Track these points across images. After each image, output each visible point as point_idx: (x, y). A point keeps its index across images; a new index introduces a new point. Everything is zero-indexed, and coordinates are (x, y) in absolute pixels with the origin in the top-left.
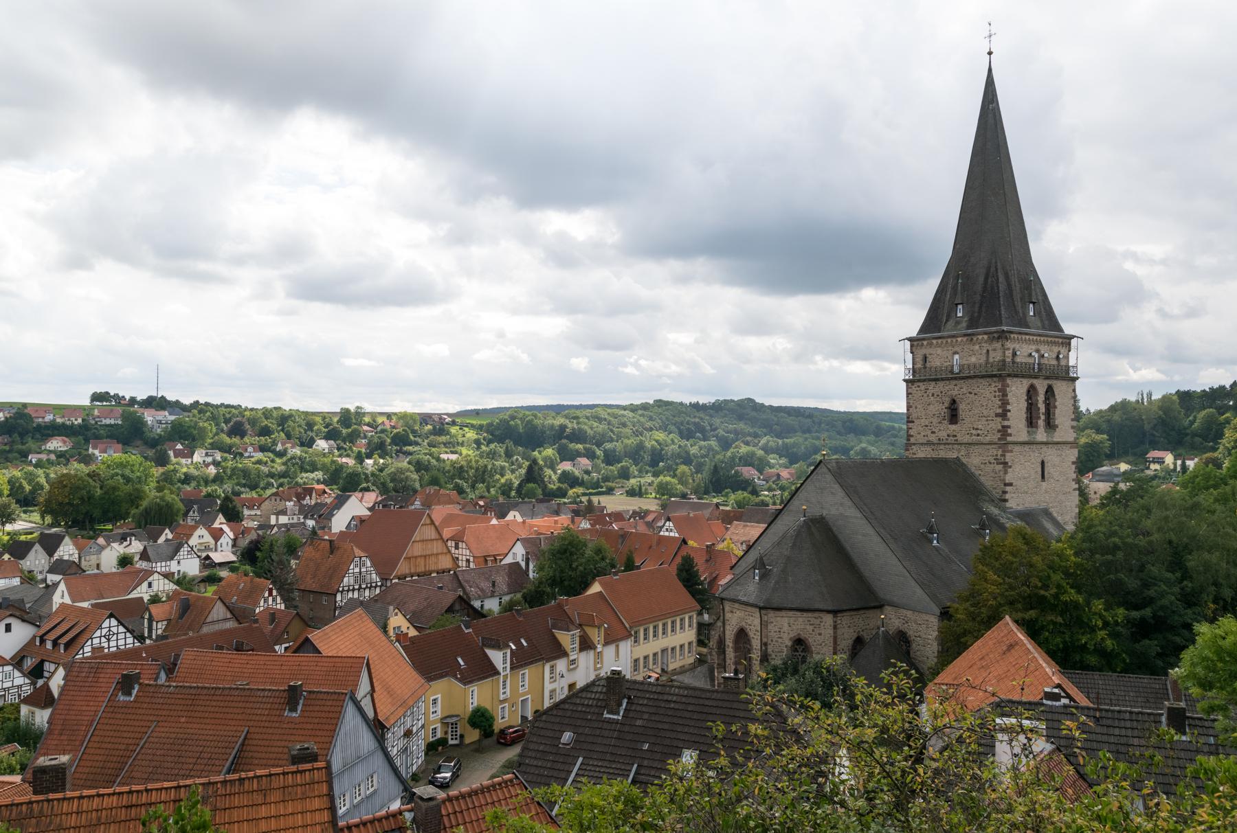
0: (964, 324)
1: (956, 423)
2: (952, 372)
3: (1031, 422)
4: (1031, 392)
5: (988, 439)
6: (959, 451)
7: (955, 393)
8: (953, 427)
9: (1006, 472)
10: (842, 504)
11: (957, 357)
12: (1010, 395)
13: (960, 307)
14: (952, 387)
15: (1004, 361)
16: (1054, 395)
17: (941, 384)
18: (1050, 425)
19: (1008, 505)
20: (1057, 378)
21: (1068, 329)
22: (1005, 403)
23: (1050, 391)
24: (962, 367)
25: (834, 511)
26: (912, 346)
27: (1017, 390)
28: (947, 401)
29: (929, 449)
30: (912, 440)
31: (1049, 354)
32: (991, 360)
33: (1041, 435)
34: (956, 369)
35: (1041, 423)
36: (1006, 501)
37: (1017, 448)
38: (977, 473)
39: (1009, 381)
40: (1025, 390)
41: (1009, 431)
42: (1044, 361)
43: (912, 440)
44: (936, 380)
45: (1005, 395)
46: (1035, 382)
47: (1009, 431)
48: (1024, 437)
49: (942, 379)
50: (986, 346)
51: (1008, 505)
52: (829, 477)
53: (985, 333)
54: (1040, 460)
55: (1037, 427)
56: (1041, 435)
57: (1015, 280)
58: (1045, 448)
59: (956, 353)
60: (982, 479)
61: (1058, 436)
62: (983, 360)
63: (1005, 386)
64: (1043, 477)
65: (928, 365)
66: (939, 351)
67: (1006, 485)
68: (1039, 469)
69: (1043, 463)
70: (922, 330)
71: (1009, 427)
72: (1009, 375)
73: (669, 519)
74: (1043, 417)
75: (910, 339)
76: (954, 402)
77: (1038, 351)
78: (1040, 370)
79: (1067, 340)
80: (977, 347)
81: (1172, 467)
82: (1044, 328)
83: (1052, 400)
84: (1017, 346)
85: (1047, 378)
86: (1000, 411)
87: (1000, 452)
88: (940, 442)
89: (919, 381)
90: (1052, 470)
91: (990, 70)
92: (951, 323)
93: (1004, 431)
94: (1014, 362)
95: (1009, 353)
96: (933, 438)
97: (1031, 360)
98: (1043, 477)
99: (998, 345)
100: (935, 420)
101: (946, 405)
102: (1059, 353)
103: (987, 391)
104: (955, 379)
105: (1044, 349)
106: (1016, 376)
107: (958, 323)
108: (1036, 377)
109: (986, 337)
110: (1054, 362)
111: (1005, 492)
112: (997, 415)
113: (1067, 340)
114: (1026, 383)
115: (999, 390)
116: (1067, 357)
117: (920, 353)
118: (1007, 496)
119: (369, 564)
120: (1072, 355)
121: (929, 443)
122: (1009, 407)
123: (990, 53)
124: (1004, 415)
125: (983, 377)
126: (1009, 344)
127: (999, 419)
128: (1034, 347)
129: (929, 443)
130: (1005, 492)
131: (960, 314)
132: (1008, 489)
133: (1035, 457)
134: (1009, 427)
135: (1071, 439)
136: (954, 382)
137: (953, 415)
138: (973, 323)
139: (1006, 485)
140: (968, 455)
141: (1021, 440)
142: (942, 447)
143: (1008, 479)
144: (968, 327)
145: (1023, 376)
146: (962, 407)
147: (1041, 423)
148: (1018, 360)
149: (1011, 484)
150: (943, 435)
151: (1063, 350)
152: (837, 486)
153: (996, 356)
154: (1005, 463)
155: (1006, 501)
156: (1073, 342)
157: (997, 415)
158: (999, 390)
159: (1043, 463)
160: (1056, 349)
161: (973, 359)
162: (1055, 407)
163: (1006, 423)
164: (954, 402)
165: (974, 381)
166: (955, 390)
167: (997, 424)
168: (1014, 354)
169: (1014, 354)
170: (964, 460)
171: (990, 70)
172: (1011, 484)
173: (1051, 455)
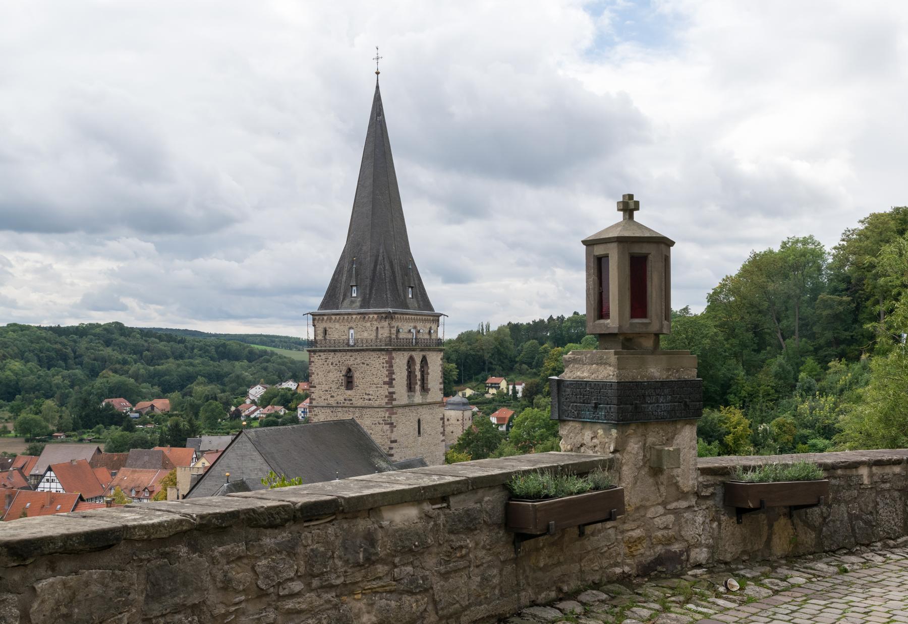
0: (358, 304)
1: (351, 389)
2: (348, 345)
3: (410, 388)
4: (411, 362)
5: (377, 403)
6: (354, 413)
7: (350, 363)
8: (349, 392)
9: (392, 432)
10: (260, 470)
11: (352, 331)
12: (395, 366)
13: (354, 288)
14: (348, 357)
15: (390, 337)
16: (427, 363)
17: (339, 354)
18: (425, 389)
19: (393, 459)
20: (429, 350)
21: (437, 311)
22: (391, 373)
24: (356, 341)
25: (253, 476)
26: (314, 320)
27: (400, 361)
28: (344, 369)
29: (328, 411)
30: (314, 403)
31: (423, 328)
32: (380, 336)
33: (418, 398)
34: (351, 343)
35: (418, 387)
36: (392, 455)
37: (400, 411)
38: (369, 432)
39: (394, 354)
40: (405, 361)
41: (394, 396)
42: (420, 336)
43: (314, 403)
44: (335, 351)
45: (391, 366)
46: (413, 353)
47: (394, 396)
49: (340, 351)
50: (376, 324)
51: (393, 459)
52: (249, 446)
53: (375, 313)
55: (414, 391)
56: (418, 398)
57: (397, 269)
58: (420, 409)
59: (351, 328)
60: (373, 437)
62: (373, 336)
63: (392, 358)
64: (419, 432)
65: (328, 337)
66: (337, 326)
67: (392, 442)
69: (419, 421)
70: (324, 306)
71: (394, 393)
72: (394, 350)
73: (50, 469)
74: (419, 383)
75: (313, 315)
76: (349, 370)
77: (415, 327)
79: (436, 318)
80: (368, 324)
81: (505, 391)
82: (420, 308)
83: (425, 368)
84: (400, 324)
85: (422, 350)
86: (387, 379)
87: (387, 415)
88: (338, 406)
89: (320, 351)
91: (378, 87)
92: (347, 301)
93: (391, 396)
94: (397, 338)
95: (394, 331)
96: (332, 402)
97: (410, 336)
98: (419, 432)
99: (386, 324)
100: (334, 386)
101: (344, 373)
102: (430, 328)
103: (377, 362)
104: (351, 351)
105: (420, 326)
106: (399, 350)
107: (352, 302)
108: (414, 350)
109: (376, 316)
110: (427, 337)
111: (391, 448)
112: (385, 383)
113: (436, 318)
114: (406, 355)
115: (387, 362)
116: (436, 332)
117: (321, 326)
118: (392, 452)
120: (440, 329)
121: (329, 406)
122: (394, 376)
123: (378, 73)
124: (390, 383)
125: (374, 350)
126: (394, 324)
127: (387, 386)
128: (412, 325)
129: (329, 406)
130: (391, 448)
131: (354, 295)
132: (394, 445)
134: (394, 393)
135: (439, 400)
136: (349, 354)
137: (349, 382)
138: (365, 303)
139: (392, 442)
140: (361, 417)
142: (340, 409)
144: (361, 307)
145: (405, 350)
146: (356, 375)
147: (418, 387)
148: (401, 336)
149: (395, 441)
150: (340, 399)
151: (434, 326)
152: (256, 453)
153: (384, 333)
154: (392, 424)
155: (392, 455)
156: (441, 318)
157: (385, 383)
158: (387, 362)
159: (419, 421)
160: (428, 325)
161: (365, 335)
162: (428, 374)
163: (391, 390)
164: (349, 370)
165: (366, 353)
166: (351, 360)
167: (385, 390)
168: (398, 331)
169: (398, 331)
170: (358, 421)
171: (378, 87)
172: (395, 441)
173: (425, 414)
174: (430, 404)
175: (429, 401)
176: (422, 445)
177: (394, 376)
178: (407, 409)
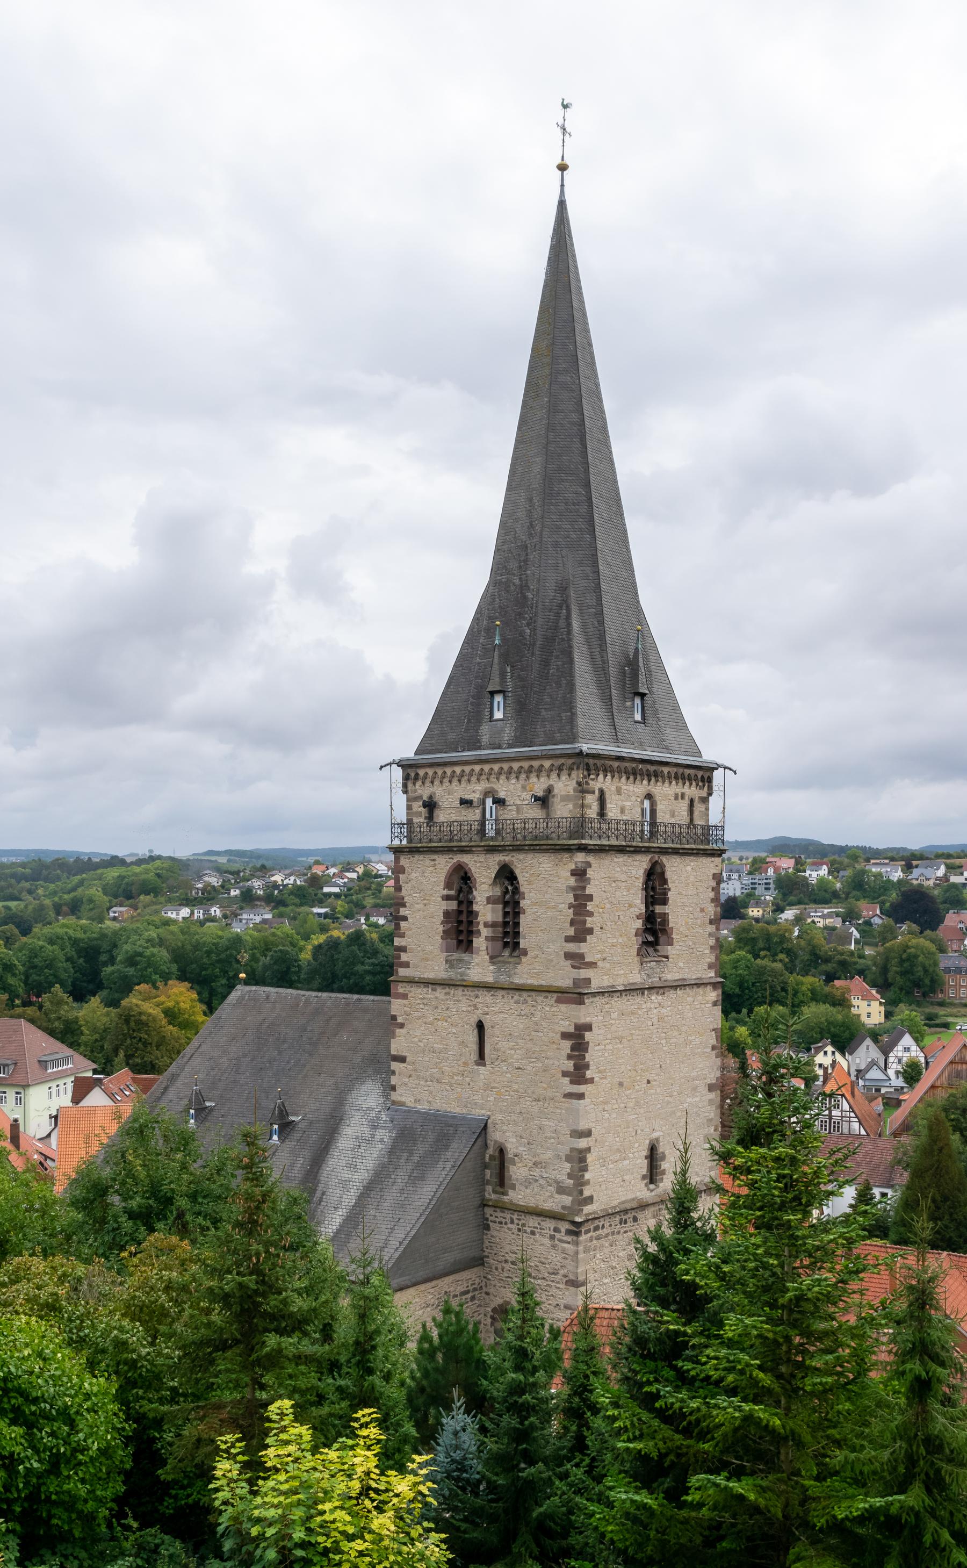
20: (518, 848)
23: (507, 875)
39: (404, 861)
41: (404, 957)
42: (509, 814)
46: (466, 859)
48: (437, 969)
54: (474, 1020)
58: (485, 998)
61: (524, 973)
64: (481, 1055)
68: (473, 1037)
69: (480, 1026)
78: (498, 832)
90: (504, 1045)
98: (481, 1055)
102: (549, 790)
110: (536, 812)
114: (444, 864)
119: (846, 1106)
122: (403, 912)
133: (460, 1011)
141: (431, 975)
143: (396, 1046)
149: (402, 1059)
159: (480, 1026)
172: (402, 1059)
173: (503, 1014)
174: (520, 989)
175: (518, 980)
176: (488, 1087)
177: (403, 912)
178: (440, 993)
